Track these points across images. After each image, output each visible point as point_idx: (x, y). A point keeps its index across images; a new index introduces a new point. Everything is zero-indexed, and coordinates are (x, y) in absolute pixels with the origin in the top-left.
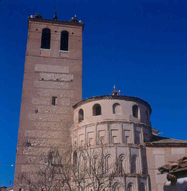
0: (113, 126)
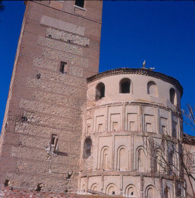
0: (147, 110)
